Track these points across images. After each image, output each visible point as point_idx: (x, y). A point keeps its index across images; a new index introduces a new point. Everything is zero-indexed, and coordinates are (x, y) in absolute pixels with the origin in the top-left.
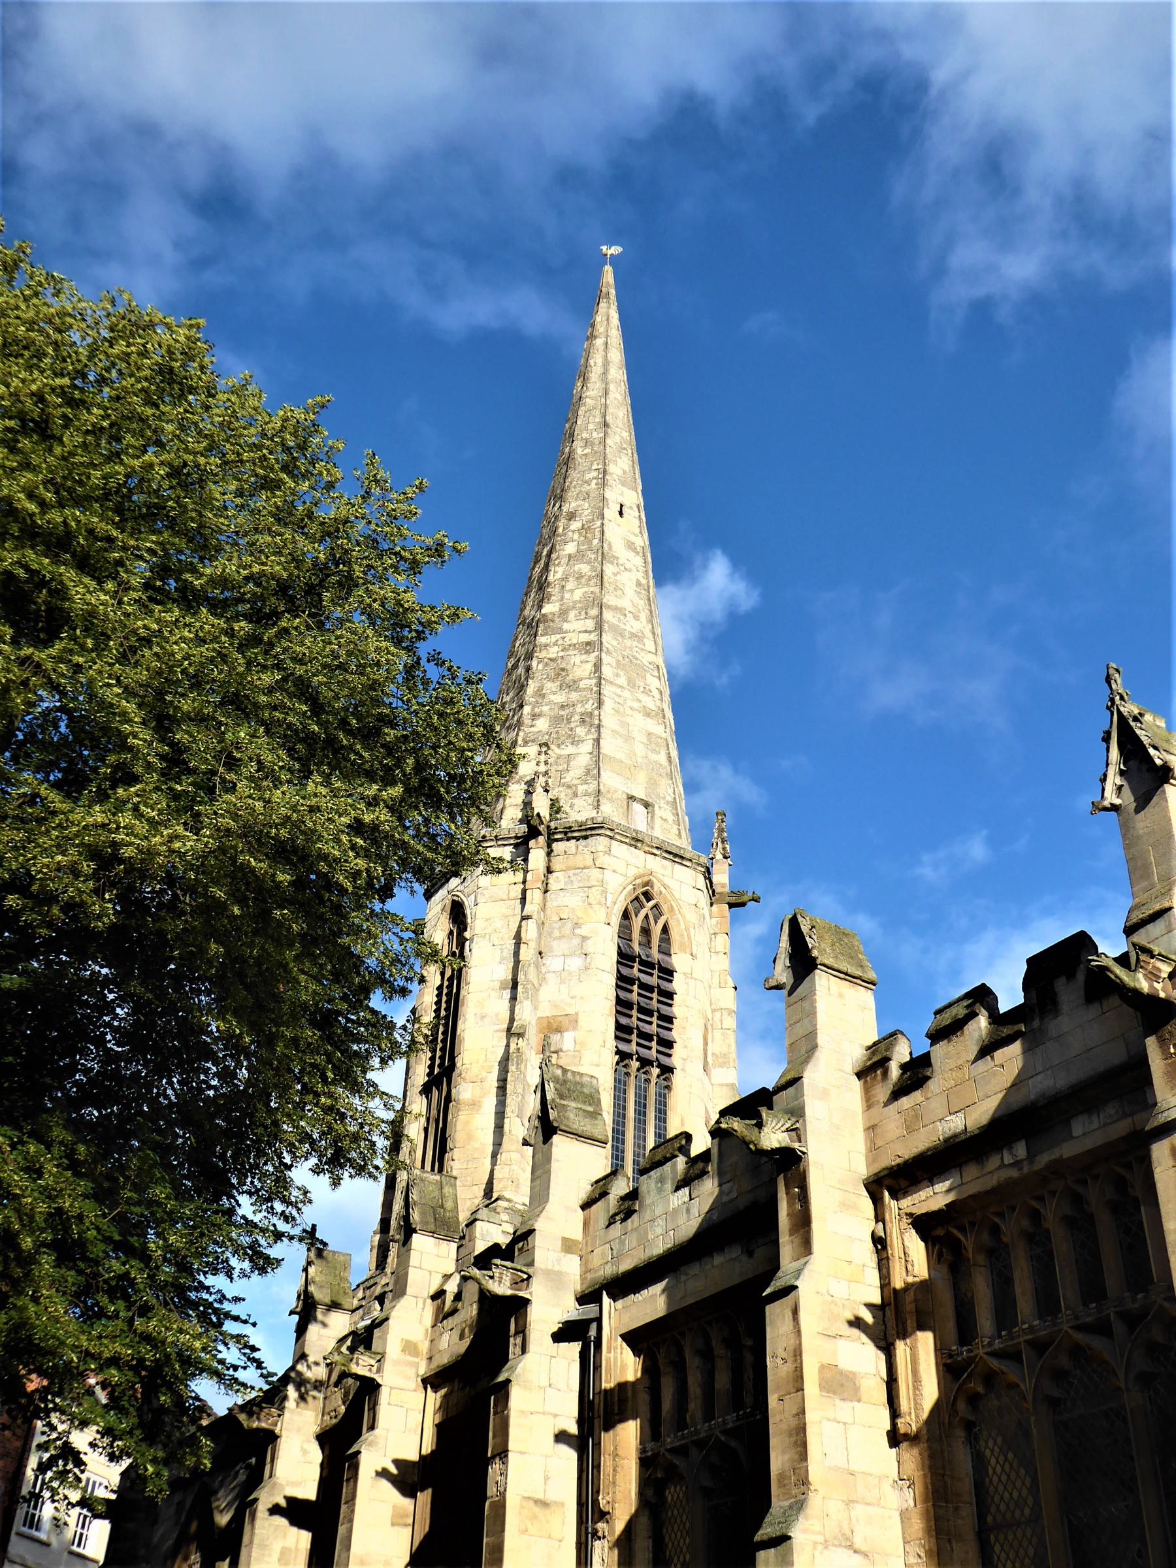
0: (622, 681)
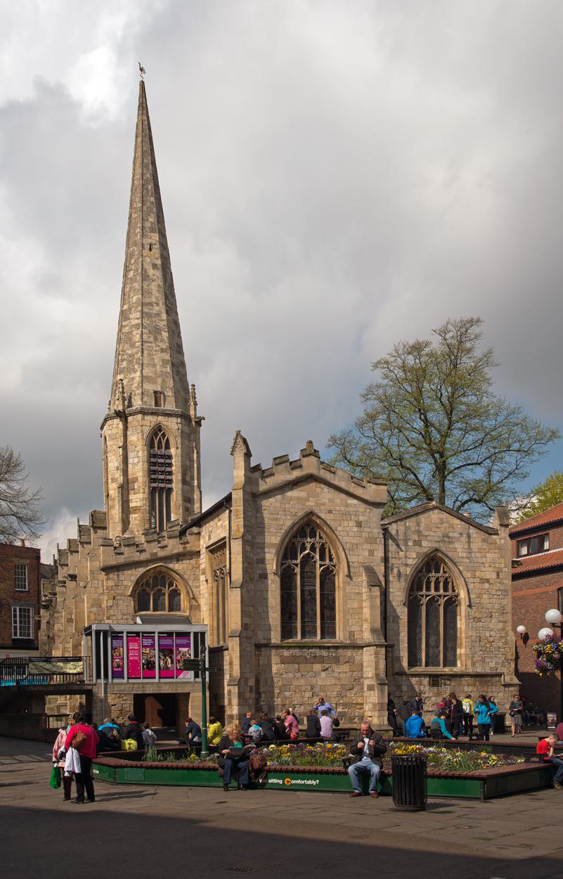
0: (152, 339)
